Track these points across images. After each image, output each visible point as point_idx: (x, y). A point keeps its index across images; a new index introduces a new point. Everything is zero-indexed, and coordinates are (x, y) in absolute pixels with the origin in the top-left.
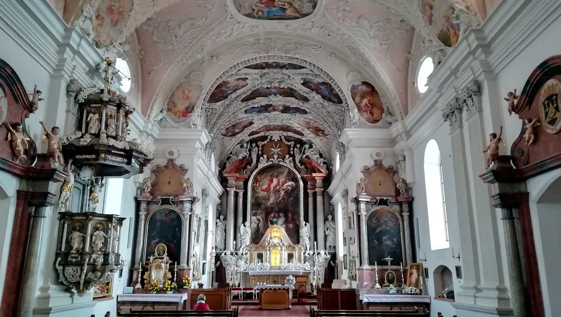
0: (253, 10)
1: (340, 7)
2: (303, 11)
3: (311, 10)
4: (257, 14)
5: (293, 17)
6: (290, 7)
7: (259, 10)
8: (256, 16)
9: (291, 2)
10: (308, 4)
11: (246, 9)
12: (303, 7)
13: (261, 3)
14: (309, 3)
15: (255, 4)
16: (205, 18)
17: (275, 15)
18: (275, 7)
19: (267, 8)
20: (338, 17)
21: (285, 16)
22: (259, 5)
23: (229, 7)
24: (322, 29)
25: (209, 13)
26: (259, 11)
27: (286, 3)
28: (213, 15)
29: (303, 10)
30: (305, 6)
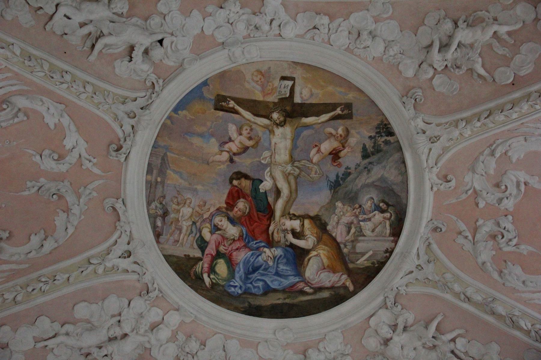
0: (202, 244)
1: (480, 222)
2: (363, 254)
3: (388, 245)
4: (212, 270)
5: (326, 294)
6: (319, 240)
7: (222, 249)
8: (205, 276)
9: (325, 218)
10: (378, 217)
11: (180, 230)
12: (360, 232)
13: (231, 214)
14: (383, 211)
15: (212, 216)
16: (42, 235)
17: (268, 291)
18: (271, 243)
19: (245, 246)
20: (480, 261)
21: (302, 292)
22: (224, 223)
23: (129, 204)
24: (426, 327)
25: (60, 220)
26: (219, 255)
27: (307, 222)
28: (71, 231)
29: (360, 247)
30: (367, 227)
